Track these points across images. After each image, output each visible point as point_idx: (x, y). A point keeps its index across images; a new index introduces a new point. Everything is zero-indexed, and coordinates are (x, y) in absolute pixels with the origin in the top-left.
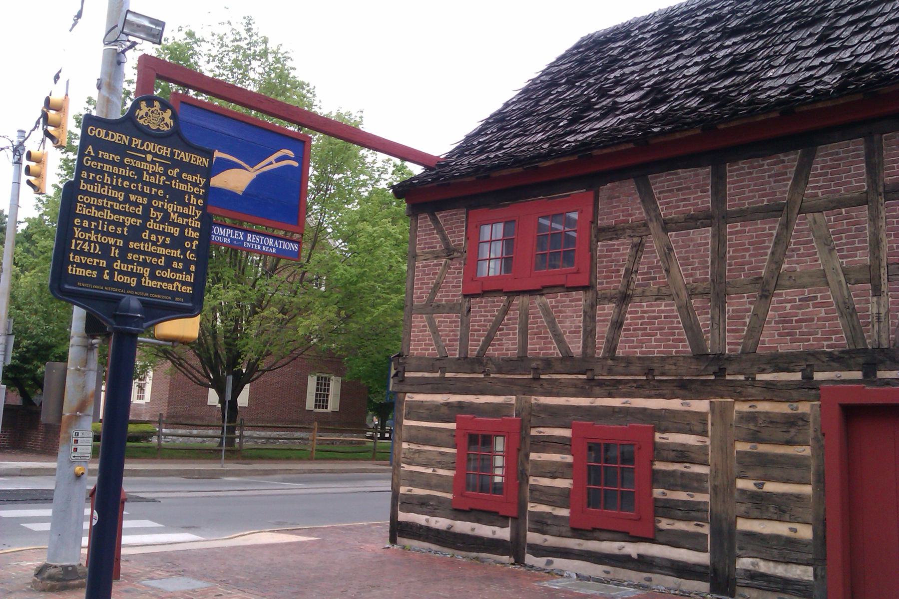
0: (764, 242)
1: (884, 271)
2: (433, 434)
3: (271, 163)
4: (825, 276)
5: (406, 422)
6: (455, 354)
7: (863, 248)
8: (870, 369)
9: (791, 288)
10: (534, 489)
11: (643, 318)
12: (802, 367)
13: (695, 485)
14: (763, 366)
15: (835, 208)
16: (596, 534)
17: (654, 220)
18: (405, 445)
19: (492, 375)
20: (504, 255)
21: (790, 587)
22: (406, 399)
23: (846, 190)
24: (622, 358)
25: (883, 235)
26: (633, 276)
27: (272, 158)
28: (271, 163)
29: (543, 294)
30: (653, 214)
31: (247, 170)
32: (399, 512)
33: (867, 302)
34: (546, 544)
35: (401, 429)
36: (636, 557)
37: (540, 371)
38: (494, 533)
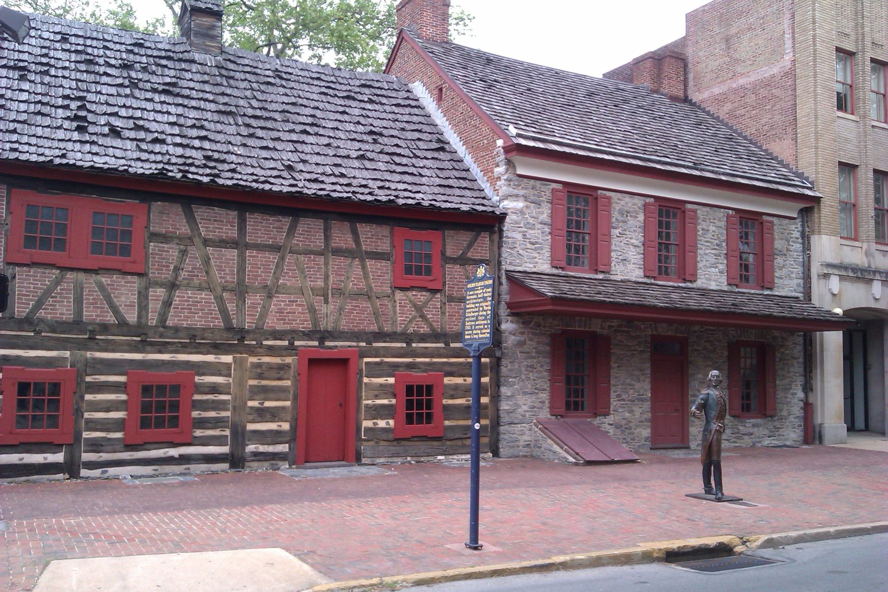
0: (270, 265)
1: (330, 292)
7: (321, 278)
8: (322, 340)
13: (221, 406)
16: (146, 447)
24: (171, 327)
25: (330, 273)
26: (180, 271)
29: (98, 274)
30: (196, 233)
33: (321, 306)
34: (101, 459)
36: (177, 457)
38: (45, 459)
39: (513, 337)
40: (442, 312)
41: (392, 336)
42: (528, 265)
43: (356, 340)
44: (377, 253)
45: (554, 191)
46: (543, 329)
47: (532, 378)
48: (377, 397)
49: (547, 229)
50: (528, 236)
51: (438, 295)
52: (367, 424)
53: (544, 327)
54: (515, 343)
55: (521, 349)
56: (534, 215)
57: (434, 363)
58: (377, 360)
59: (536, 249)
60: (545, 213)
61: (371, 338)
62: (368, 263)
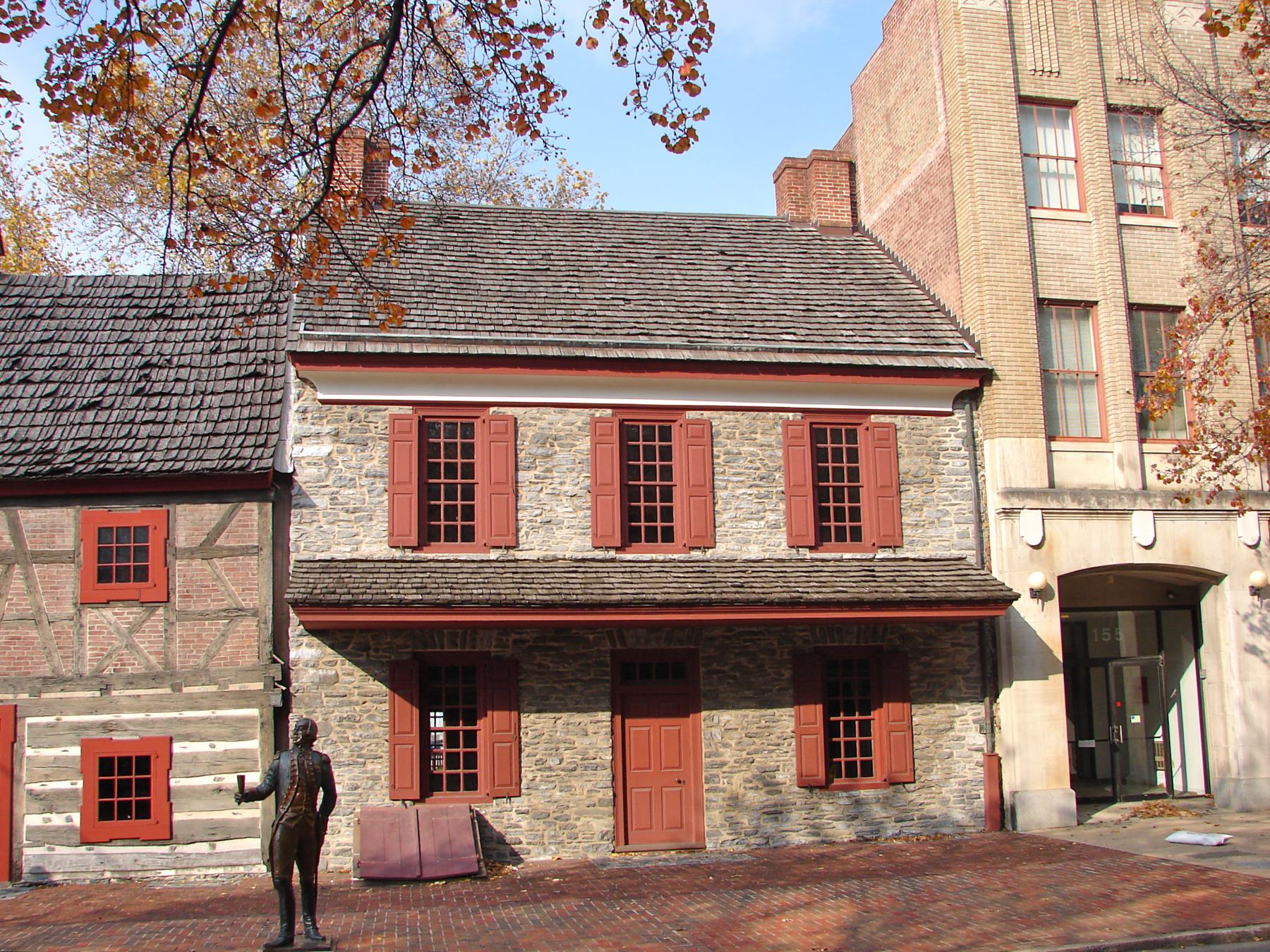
39: (312, 671)
40: (166, 638)
41: (78, 680)
42: (342, 548)
43: (12, 690)
44: (51, 554)
45: (394, 418)
46: (372, 653)
47: (351, 738)
48: (48, 778)
49: (380, 485)
50: (341, 500)
51: (161, 611)
52: (33, 820)
53: (376, 650)
54: (317, 680)
55: (329, 691)
56: (354, 463)
57: (154, 722)
58: (52, 719)
59: (358, 520)
60: (377, 457)
61: (39, 686)
62: (36, 569)
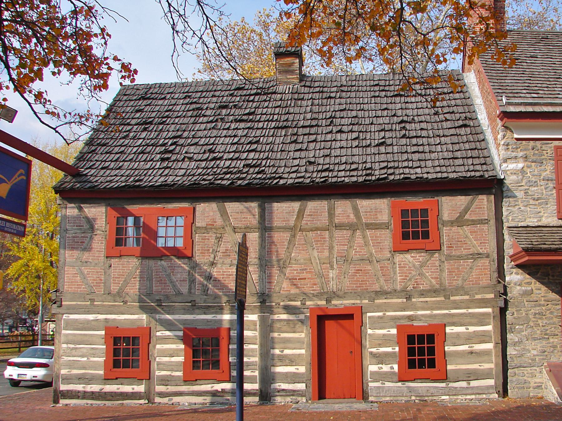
0: (284, 242)
1: (335, 260)
2: (86, 338)
3: (16, 179)
4: (311, 260)
5: (64, 332)
6: (101, 291)
7: (327, 249)
8: (328, 301)
9: (296, 264)
10: (159, 364)
11: (224, 275)
12: (301, 300)
13: (251, 354)
14: (284, 299)
15: (315, 231)
16: (198, 382)
17: (228, 226)
18: (64, 346)
19: (129, 303)
20: (135, 236)
21: (296, 393)
22: (64, 317)
23: (320, 223)
24: (211, 295)
25: (335, 245)
26: (217, 253)
27: (16, 176)
28: (16, 179)
29: (162, 260)
30: (227, 223)
31: (7, 183)
32: (61, 385)
33: (328, 272)
34: (168, 390)
35: (61, 336)
36: (221, 390)
37: (162, 301)
38: (133, 389)
39: (518, 288)
40: (440, 270)
41: (393, 293)
42: (531, 220)
43: (359, 298)
44: (376, 224)
45: (557, 148)
46: (551, 277)
47: (541, 324)
48: (380, 345)
49: (551, 185)
50: (530, 193)
51: (437, 255)
52: (373, 368)
53: (553, 276)
54: (521, 293)
55: (528, 298)
56: (536, 173)
57: (436, 315)
58: (380, 314)
59: (540, 204)
60: (549, 169)
61: (373, 296)
62: (368, 233)
